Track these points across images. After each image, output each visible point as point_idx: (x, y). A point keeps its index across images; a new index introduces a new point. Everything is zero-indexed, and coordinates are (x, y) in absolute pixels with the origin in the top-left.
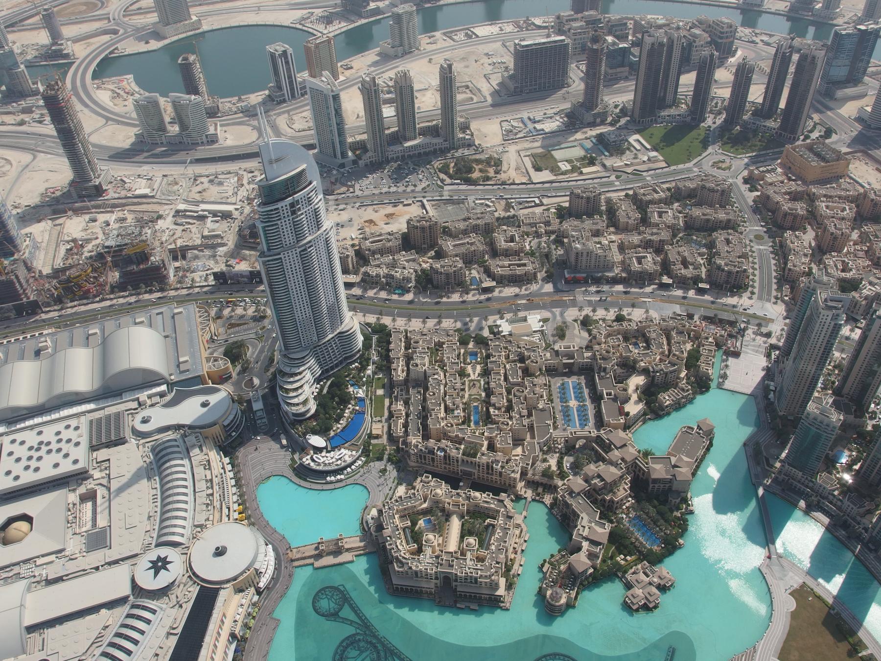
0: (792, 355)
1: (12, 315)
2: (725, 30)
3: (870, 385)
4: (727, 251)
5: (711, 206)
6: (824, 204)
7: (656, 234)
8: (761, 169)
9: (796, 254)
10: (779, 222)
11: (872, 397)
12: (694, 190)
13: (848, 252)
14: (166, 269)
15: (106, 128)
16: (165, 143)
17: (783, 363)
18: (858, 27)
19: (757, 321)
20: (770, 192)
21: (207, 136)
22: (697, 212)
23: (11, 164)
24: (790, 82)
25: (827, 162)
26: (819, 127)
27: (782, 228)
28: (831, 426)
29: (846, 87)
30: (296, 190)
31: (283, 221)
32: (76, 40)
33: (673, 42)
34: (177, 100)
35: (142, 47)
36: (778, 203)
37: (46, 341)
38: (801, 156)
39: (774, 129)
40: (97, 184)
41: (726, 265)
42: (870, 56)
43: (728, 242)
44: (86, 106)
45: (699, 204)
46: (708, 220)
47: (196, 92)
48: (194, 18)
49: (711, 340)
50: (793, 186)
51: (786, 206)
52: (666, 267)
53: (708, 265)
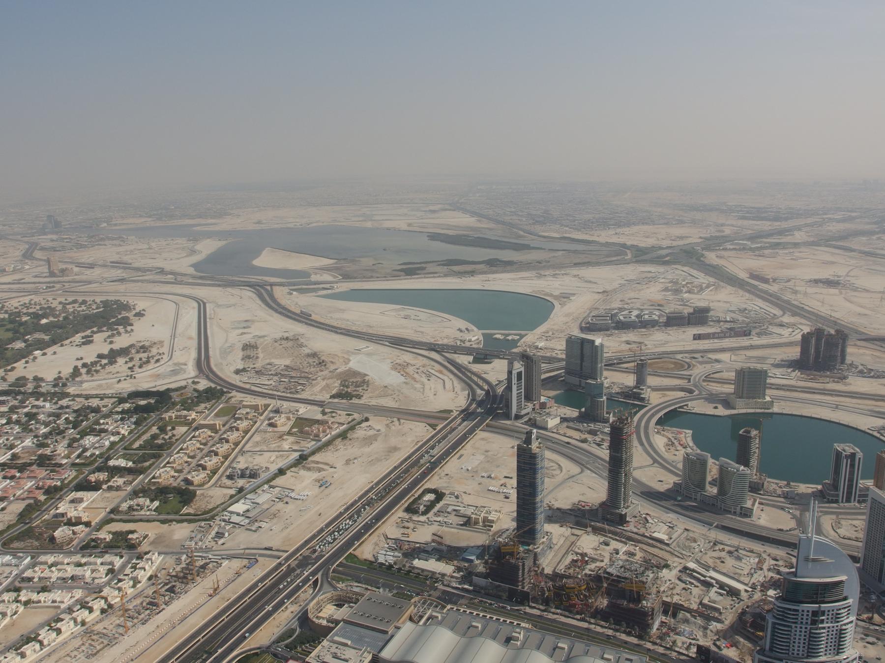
1: (505, 596)
14: (652, 619)
15: (651, 468)
16: (698, 499)
21: (742, 508)
23: (561, 471)
30: (826, 599)
31: (798, 626)
32: (655, 389)
34: (726, 465)
35: (708, 409)
37: (520, 633)
40: (623, 513)
44: (642, 444)
47: (746, 464)
48: (768, 399)
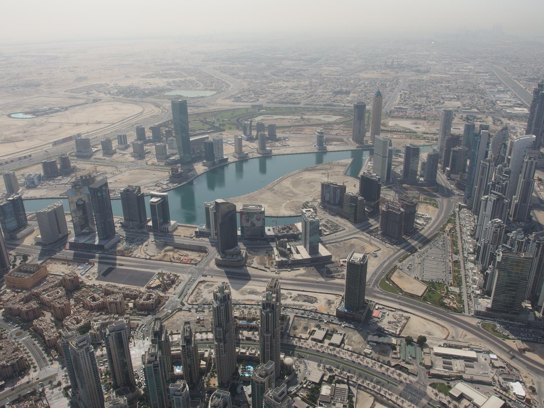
0: (79, 385)
3: (127, 372)
4: (3, 354)
6: (45, 295)
9: (47, 330)
10: (26, 318)
11: (133, 376)
13: (74, 312)
17: (77, 393)
18: (8, 199)
19: (48, 381)
20: (10, 305)
25: (33, 273)
26: (17, 257)
27: (30, 321)
29: (21, 231)
36: (18, 309)
38: (17, 277)
41: (7, 362)
42: (24, 210)
50: (22, 295)
51: (25, 308)
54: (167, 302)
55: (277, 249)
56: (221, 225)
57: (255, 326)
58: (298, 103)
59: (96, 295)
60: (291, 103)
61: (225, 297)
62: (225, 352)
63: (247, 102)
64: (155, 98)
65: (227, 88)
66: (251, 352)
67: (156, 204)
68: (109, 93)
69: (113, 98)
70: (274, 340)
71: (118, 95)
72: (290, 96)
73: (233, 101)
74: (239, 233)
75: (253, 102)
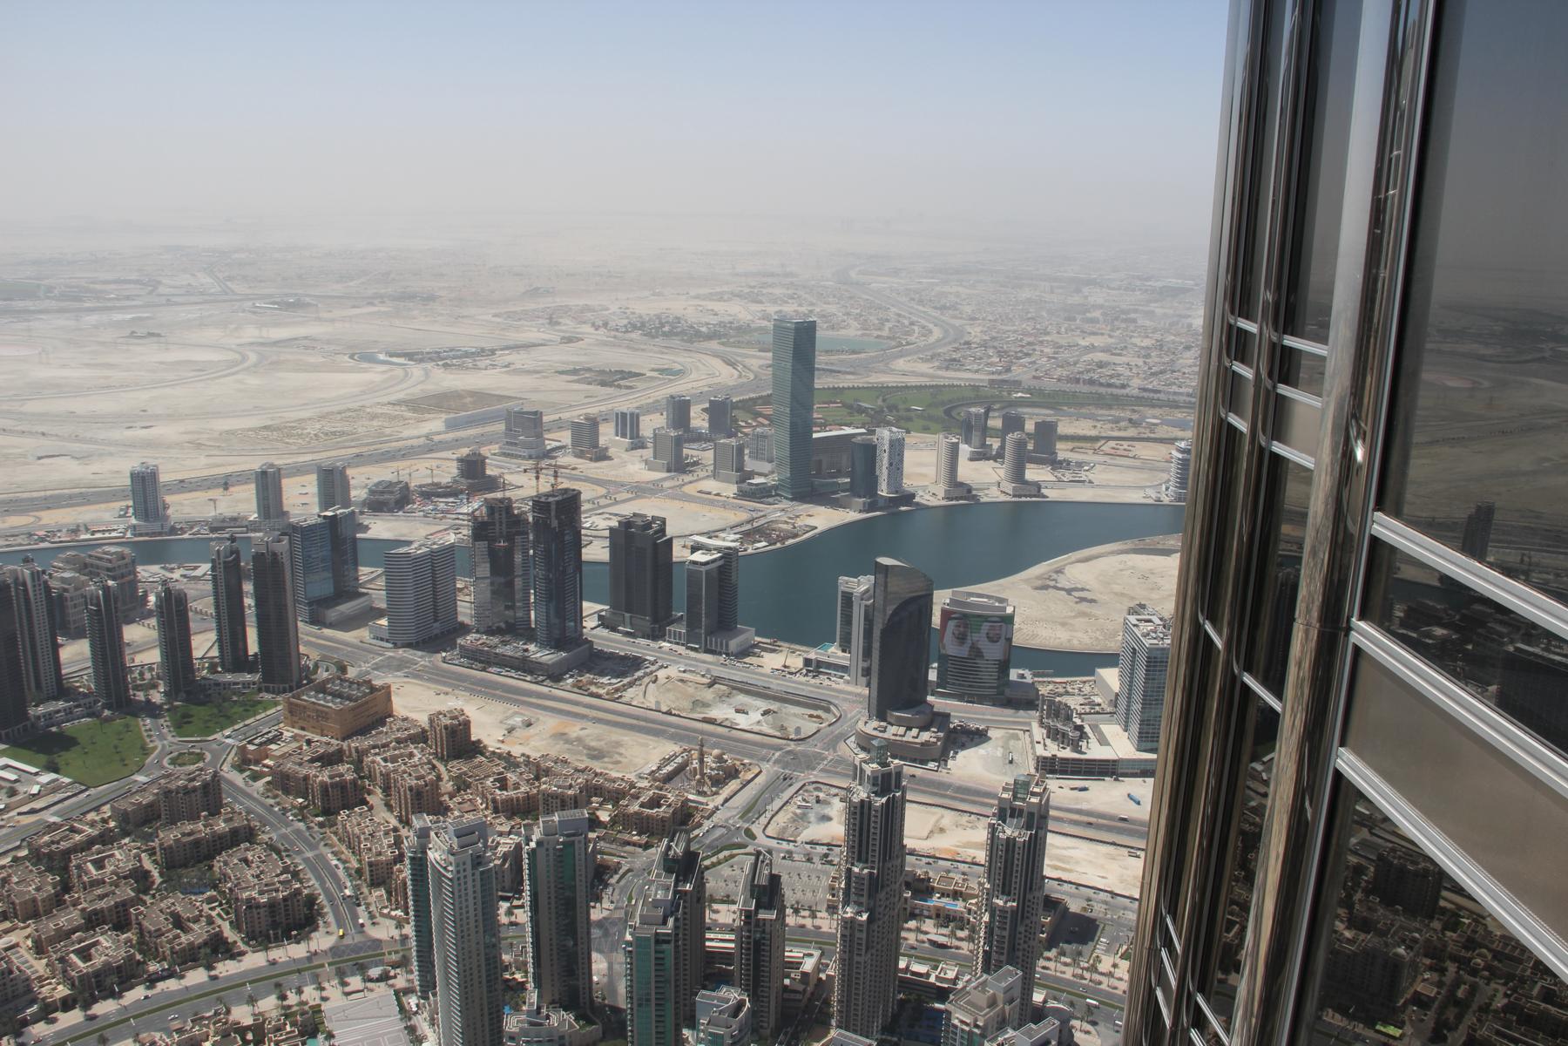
2: (115, 564)
5: (194, 818)
6: (378, 759)
7: (106, 895)
8: (257, 741)
12: (151, 805)
20: (289, 766)
22: (170, 836)
24: (254, 619)
28: (556, 1038)
33: (24, 584)
36: (306, 778)
39: (254, 683)
41: (261, 893)
42: (356, 564)
43: (246, 861)
45: (173, 821)
46: (197, 843)
49: (288, 1028)
51: (324, 776)
52: (147, 945)
53: (228, 913)
54: (707, 825)
55: (1041, 724)
56: (883, 632)
57: (958, 915)
58: (1123, 386)
59: (512, 777)
60: (1101, 385)
61: (886, 777)
62: (867, 949)
63: (977, 371)
64: (723, 344)
65: (923, 336)
66: (942, 975)
67: (703, 569)
68: (605, 325)
69: (615, 337)
70: (1021, 929)
71: (627, 332)
72: (1101, 367)
73: (939, 368)
74: (933, 676)
75: (993, 373)
